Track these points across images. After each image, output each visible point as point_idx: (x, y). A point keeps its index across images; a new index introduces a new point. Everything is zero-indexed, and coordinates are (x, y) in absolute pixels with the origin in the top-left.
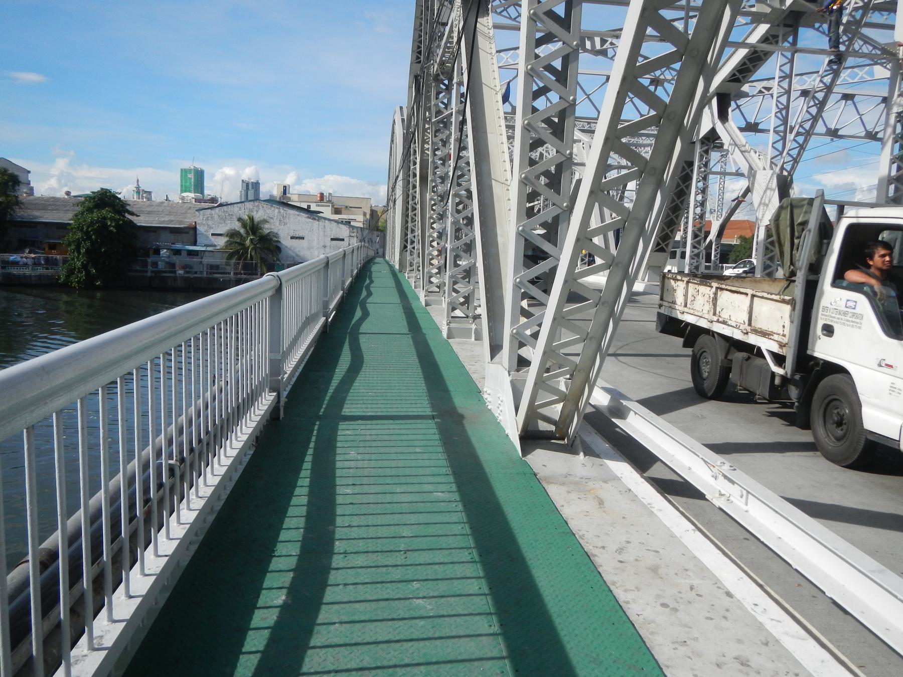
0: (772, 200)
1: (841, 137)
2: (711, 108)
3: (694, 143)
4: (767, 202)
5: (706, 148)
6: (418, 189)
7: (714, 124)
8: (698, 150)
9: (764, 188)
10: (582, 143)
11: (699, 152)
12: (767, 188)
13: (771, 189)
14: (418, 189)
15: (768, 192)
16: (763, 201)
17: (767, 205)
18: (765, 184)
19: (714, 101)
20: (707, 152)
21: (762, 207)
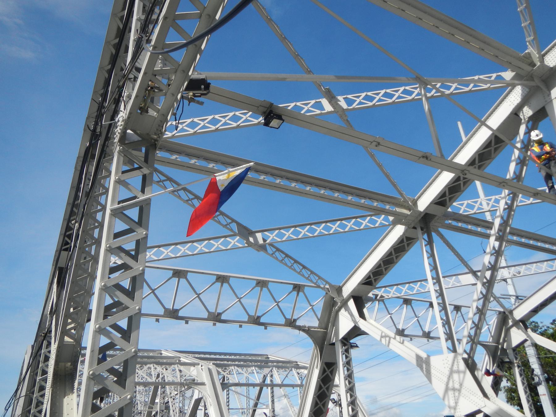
1: (432, 338)
2: (348, 309)
3: (333, 344)
4: (457, 386)
5: (346, 347)
6: (48, 392)
7: (354, 321)
8: (340, 349)
9: (447, 373)
10: (200, 366)
11: (342, 352)
12: (452, 372)
13: (458, 372)
14: (48, 392)
15: (456, 376)
16: (451, 385)
17: (459, 391)
18: (448, 369)
19: (351, 304)
20: (347, 351)
21: (451, 393)
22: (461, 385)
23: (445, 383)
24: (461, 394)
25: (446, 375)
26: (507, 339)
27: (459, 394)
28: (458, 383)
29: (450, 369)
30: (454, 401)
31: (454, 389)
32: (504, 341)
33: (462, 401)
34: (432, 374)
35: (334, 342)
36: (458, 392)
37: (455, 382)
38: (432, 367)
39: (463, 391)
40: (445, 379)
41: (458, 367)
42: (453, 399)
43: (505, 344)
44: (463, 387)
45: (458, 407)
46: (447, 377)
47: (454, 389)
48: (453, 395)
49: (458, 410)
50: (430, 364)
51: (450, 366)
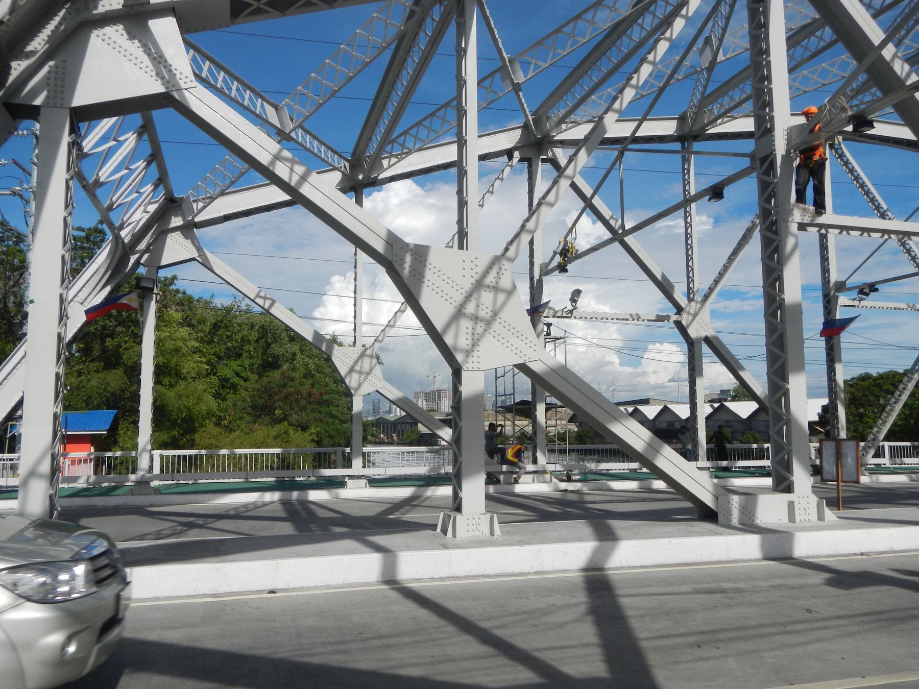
0: (504, 315)
4: (485, 313)
12: (479, 285)
15: (487, 297)
16: (470, 308)
17: (489, 323)
18: (473, 280)
22: (495, 314)
23: (457, 304)
24: (491, 331)
25: (463, 291)
26: (154, 249)
27: (485, 330)
28: (488, 311)
29: (476, 281)
30: (469, 342)
31: (476, 318)
32: (147, 250)
33: (488, 345)
34: (426, 280)
35: (38, 102)
36: (483, 325)
37: (481, 307)
38: (428, 266)
39: (496, 326)
40: (459, 298)
41: (497, 283)
42: (469, 337)
43: (146, 256)
44: (498, 320)
45: (475, 354)
46: (465, 294)
47: (476, 318)
48: (470, 330)
49: (470, 360)
50: (426, 260)
51: (476, 277)
